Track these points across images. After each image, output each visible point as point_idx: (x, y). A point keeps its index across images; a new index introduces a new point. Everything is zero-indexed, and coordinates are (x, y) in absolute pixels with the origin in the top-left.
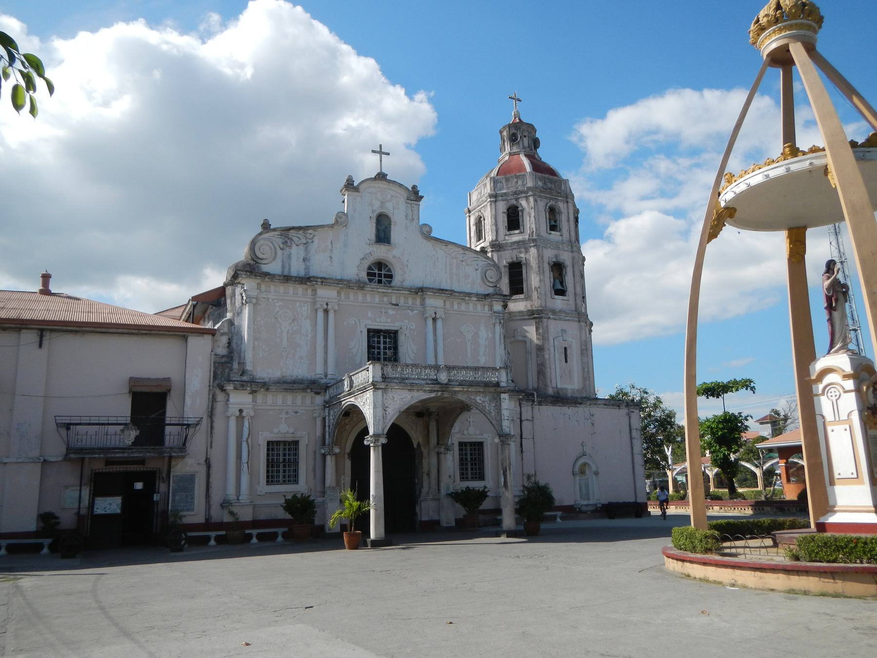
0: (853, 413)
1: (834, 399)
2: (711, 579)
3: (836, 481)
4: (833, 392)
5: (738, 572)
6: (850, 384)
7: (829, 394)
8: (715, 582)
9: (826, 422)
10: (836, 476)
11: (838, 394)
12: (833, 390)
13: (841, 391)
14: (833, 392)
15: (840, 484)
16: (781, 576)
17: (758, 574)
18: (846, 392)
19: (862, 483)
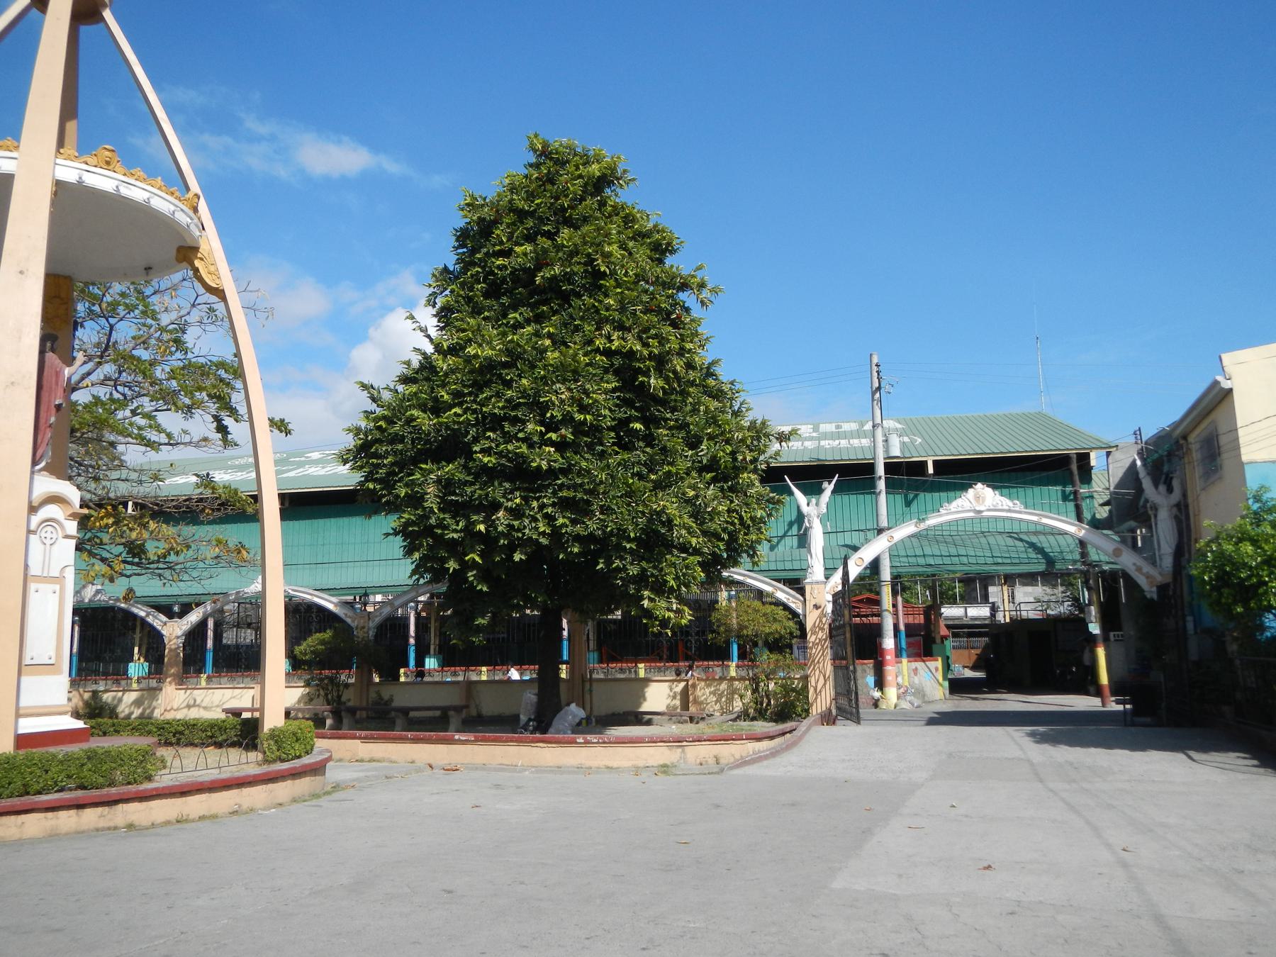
0: (68, 568)
1: (48, 542)
2: (191, 817)
3: (24, 668)
4: (48, 532)
5: (246, 791)
6: (72, 527)
7: (43, 535)
8: (202, 818)
9: (29, 577)
10: (27, 661)
11: (54, 536)
12: (49, 529)
13: (60, 534)
14: (49, 532)
15: (28, 674)
16: (289, 782)
17: (271, 786)
18: (67, 537)
19: (59, 672)
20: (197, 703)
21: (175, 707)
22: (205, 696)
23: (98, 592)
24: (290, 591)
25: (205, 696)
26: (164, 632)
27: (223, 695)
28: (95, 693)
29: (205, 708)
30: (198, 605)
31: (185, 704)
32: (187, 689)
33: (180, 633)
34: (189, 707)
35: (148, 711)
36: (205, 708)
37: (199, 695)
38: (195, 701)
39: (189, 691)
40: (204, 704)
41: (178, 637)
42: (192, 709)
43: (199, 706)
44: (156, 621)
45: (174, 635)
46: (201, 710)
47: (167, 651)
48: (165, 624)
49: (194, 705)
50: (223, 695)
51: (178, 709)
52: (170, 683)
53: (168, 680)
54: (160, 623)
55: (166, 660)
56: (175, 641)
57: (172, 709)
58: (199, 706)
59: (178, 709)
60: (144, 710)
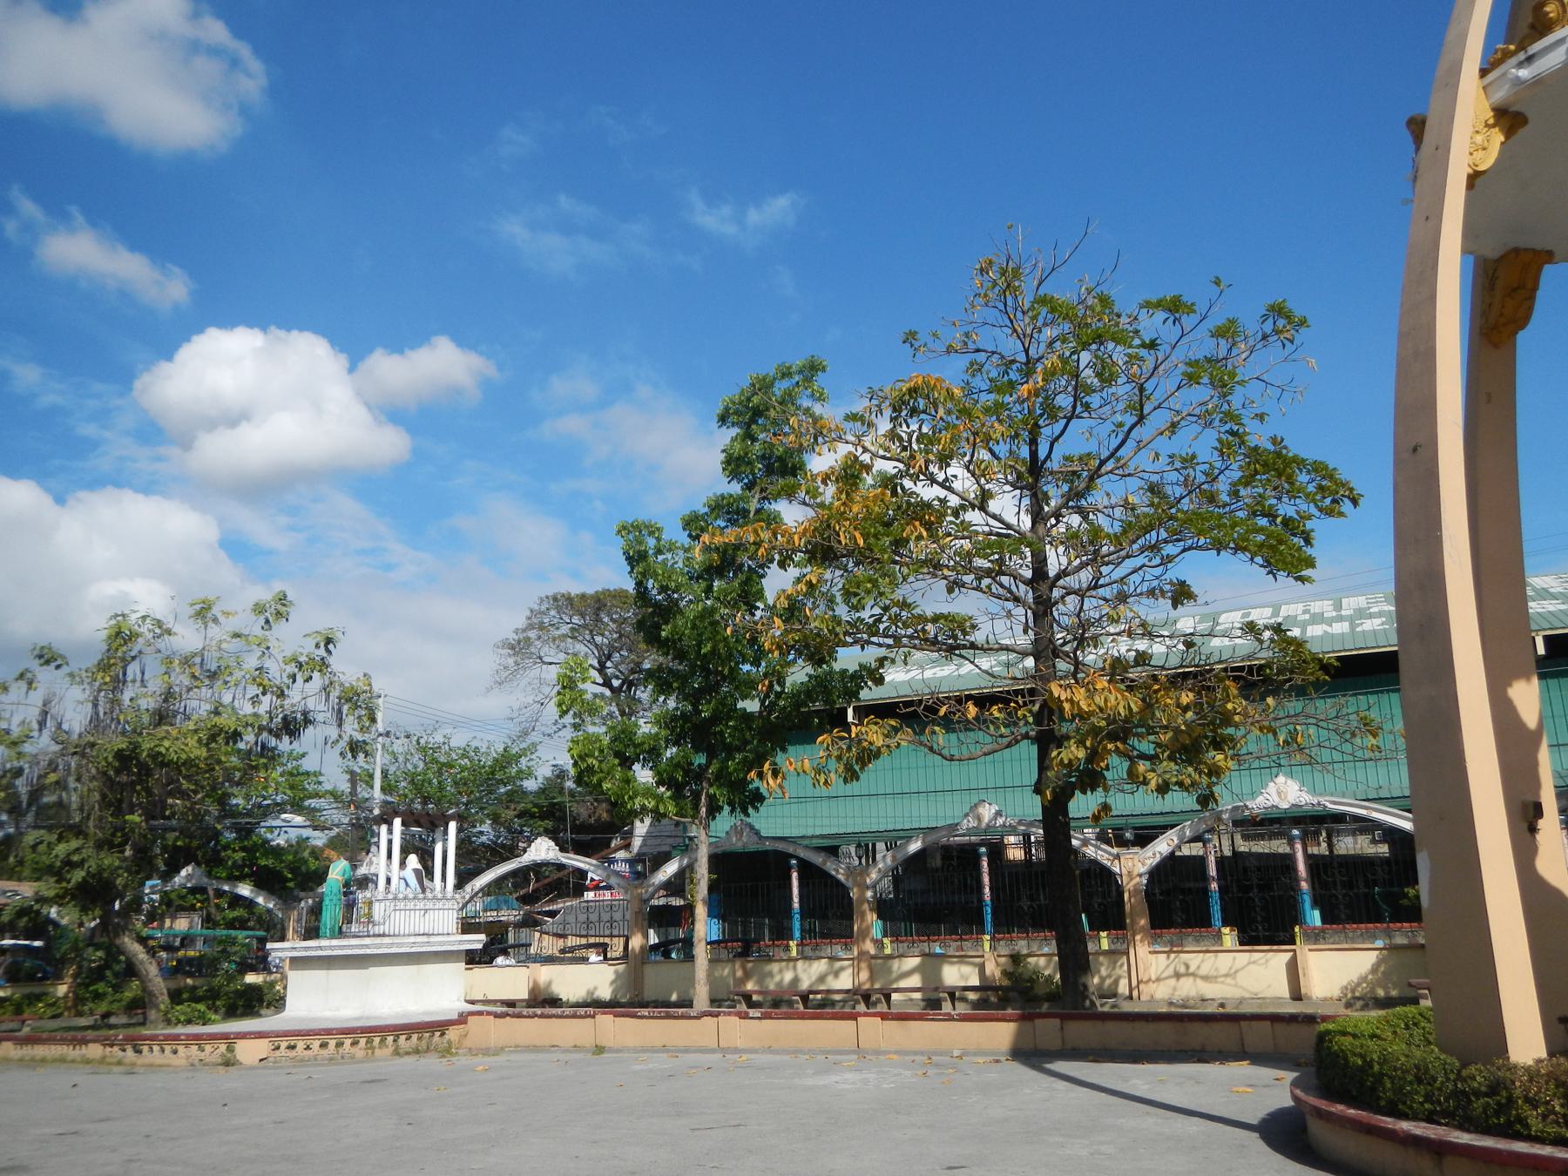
20: (1192, 970)
21: (1153, 978)
22: (1202, 961)
23: (999, 814)
24: (1327, 804)
25: (1202, 961)
26: (1117, 870)
27: (1234, 959)
28: (1016, 958)
29: (1206, 978)
30: (1165, 828)
31: (1170, 971)
32: (1171, 951)
33: (1143, 870)
34: (1178, 976)
35: (1108, 982)
36: (1206, 978)
37: (1191, 959)
38: (1187, 967)
39: (1173, 956)
40: (1203, 972)
41: (1140, 875)
42: (1183, 980)
43: (1193, 975)
44: (1099, 852)
45: (1135, 873)
46: (1198, 981)
47: (1126, 896)
48: (1118, 857)
49: (1187, 975)
50: (1234, 959)
51: (1158, 980)
52: (1141, 941)
53: (1138, 937)
54: (1106, 856)
55: (1128, 907)
56: (1138, 879)
57: (1150, 980)
58: (1193, 975)
59: (1158, 980)
60: (1103, 979)
